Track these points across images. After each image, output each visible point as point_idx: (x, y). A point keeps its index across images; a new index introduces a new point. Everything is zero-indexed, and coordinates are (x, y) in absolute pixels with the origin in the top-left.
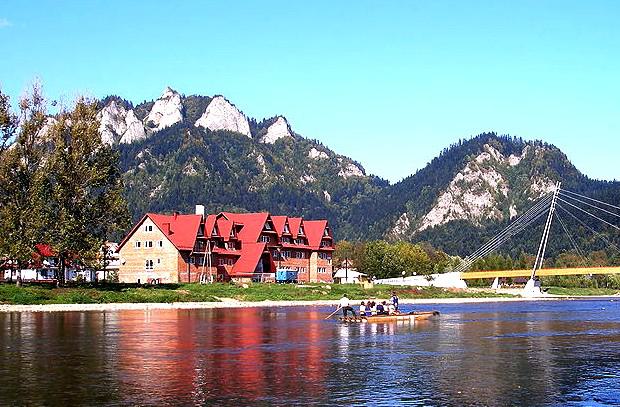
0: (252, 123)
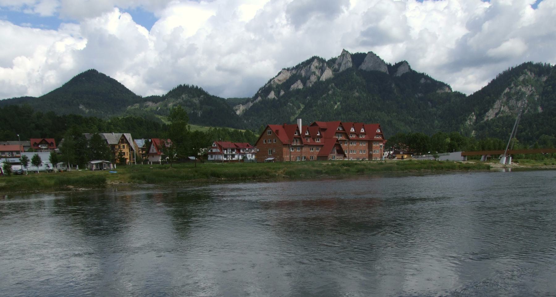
0: (389, 66)
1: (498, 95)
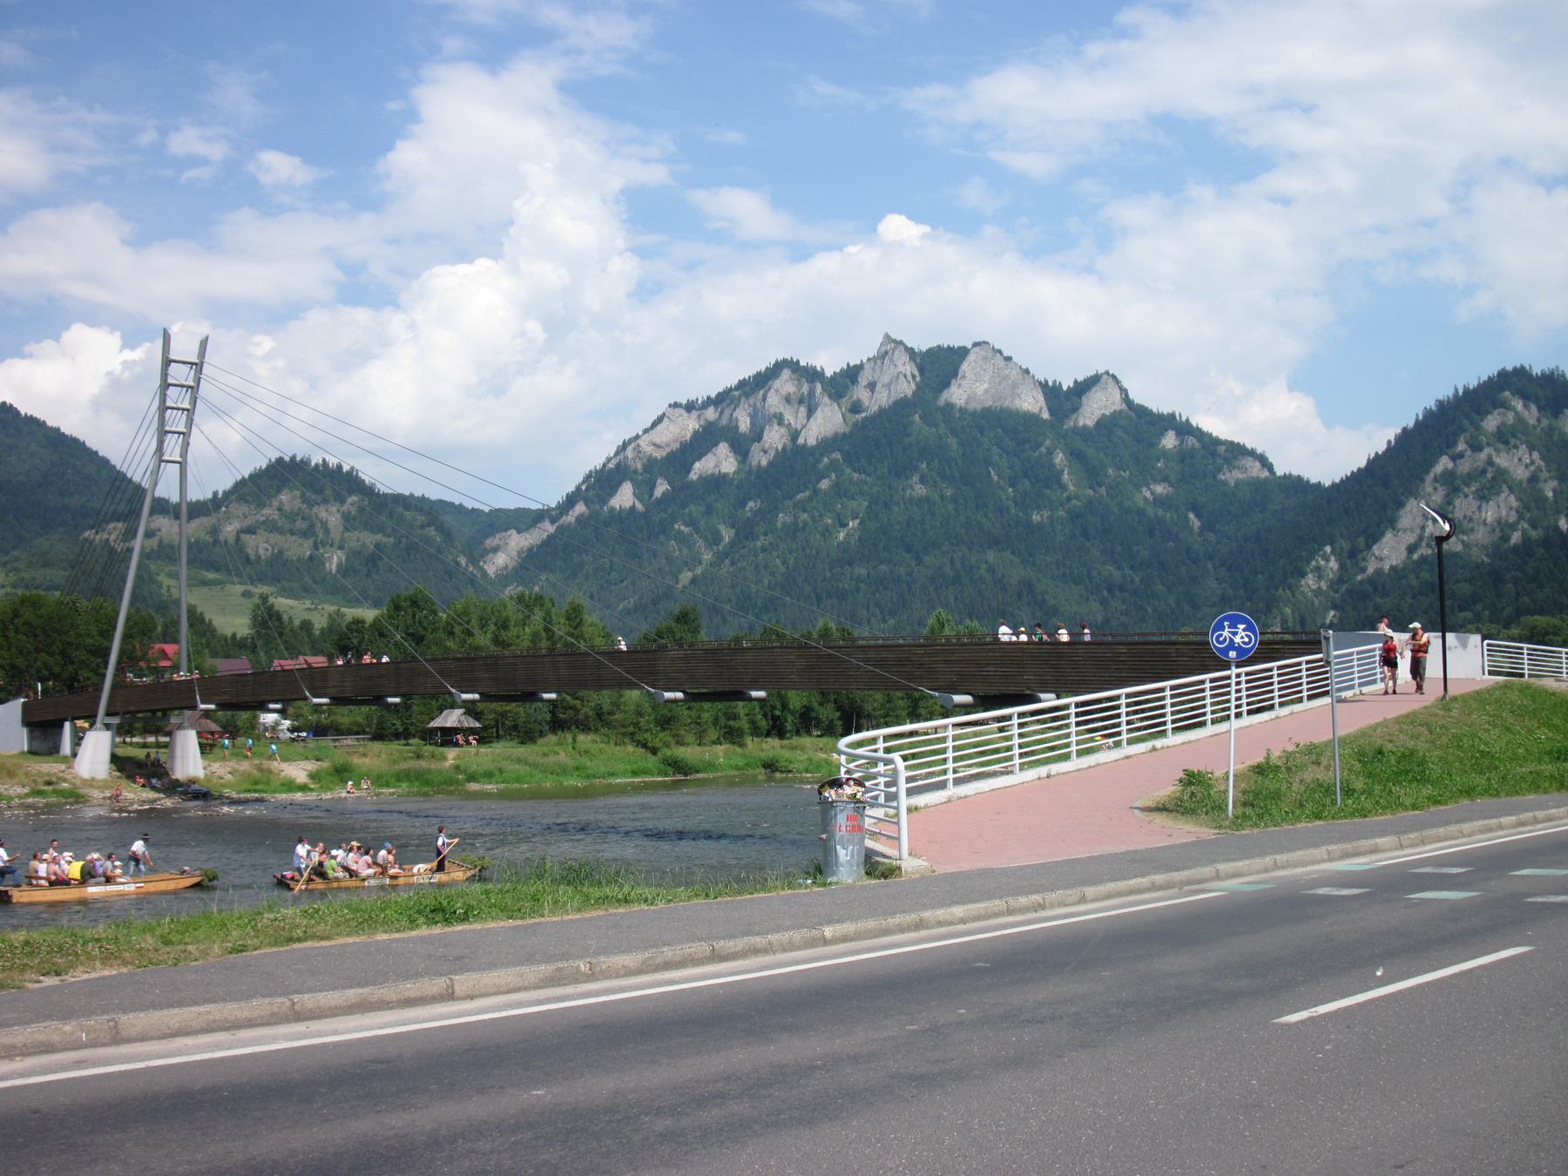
0: (1051, 392)
1: (1411, 486)
